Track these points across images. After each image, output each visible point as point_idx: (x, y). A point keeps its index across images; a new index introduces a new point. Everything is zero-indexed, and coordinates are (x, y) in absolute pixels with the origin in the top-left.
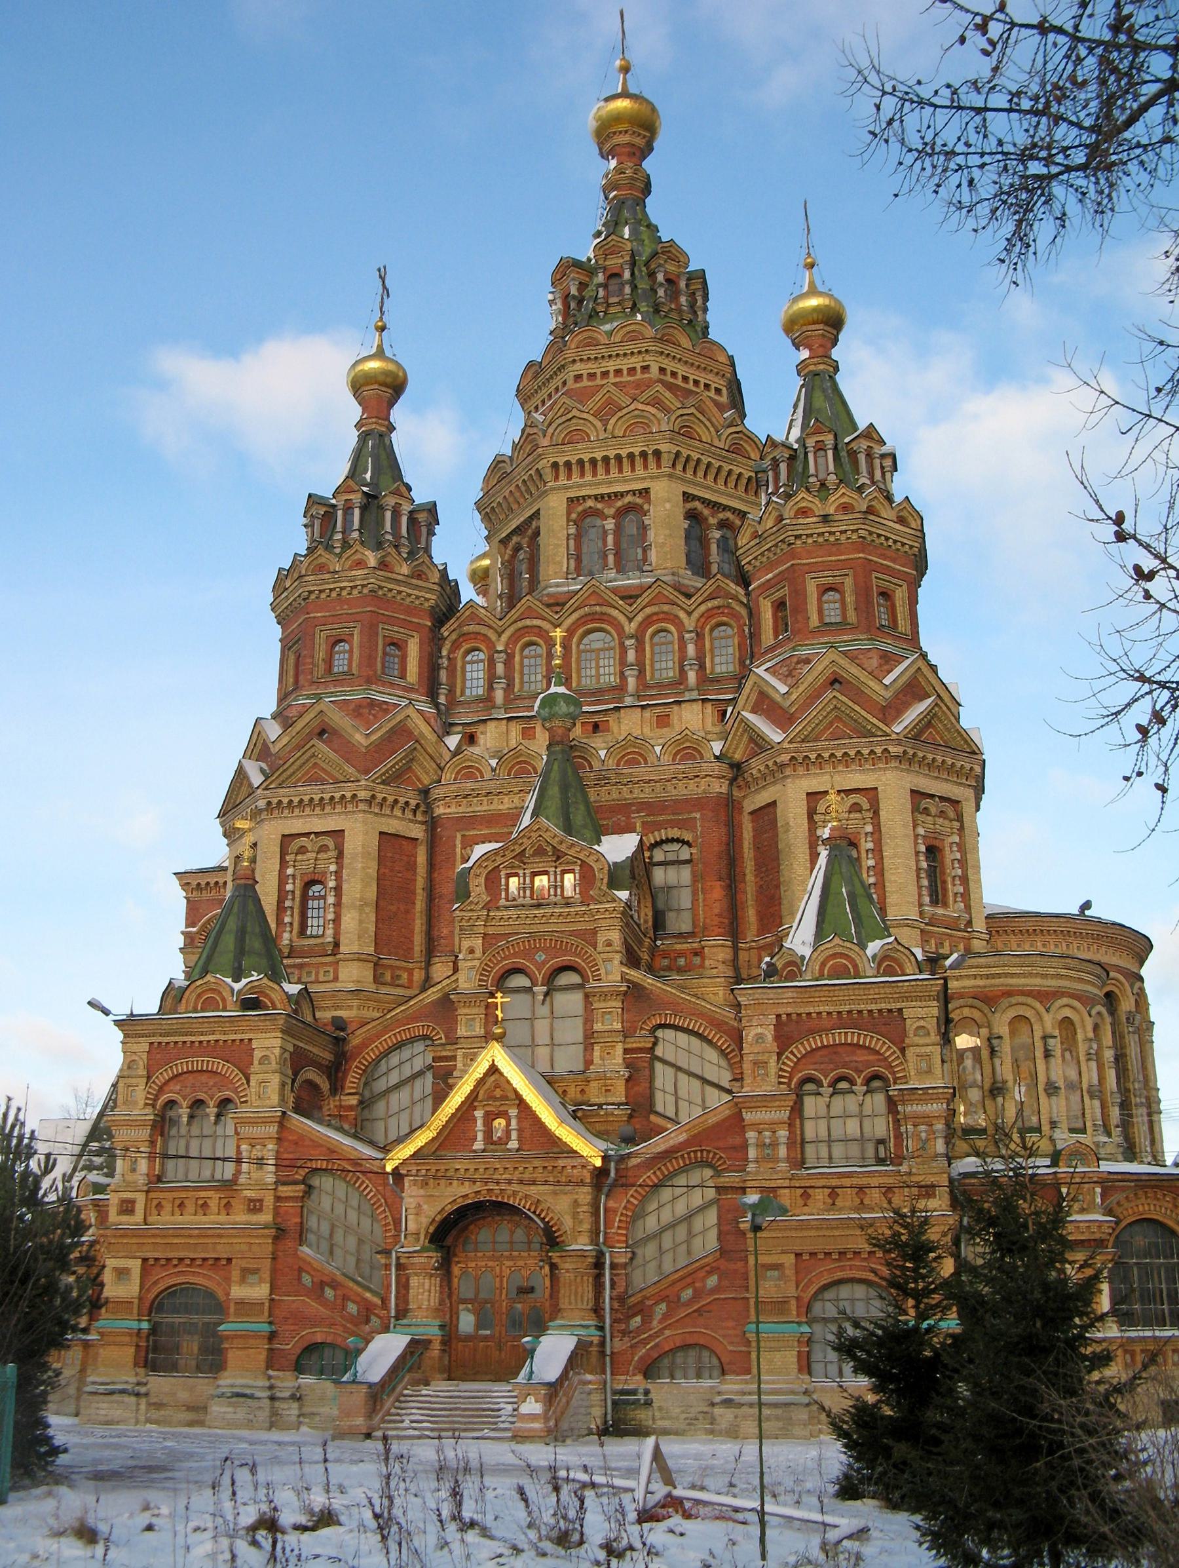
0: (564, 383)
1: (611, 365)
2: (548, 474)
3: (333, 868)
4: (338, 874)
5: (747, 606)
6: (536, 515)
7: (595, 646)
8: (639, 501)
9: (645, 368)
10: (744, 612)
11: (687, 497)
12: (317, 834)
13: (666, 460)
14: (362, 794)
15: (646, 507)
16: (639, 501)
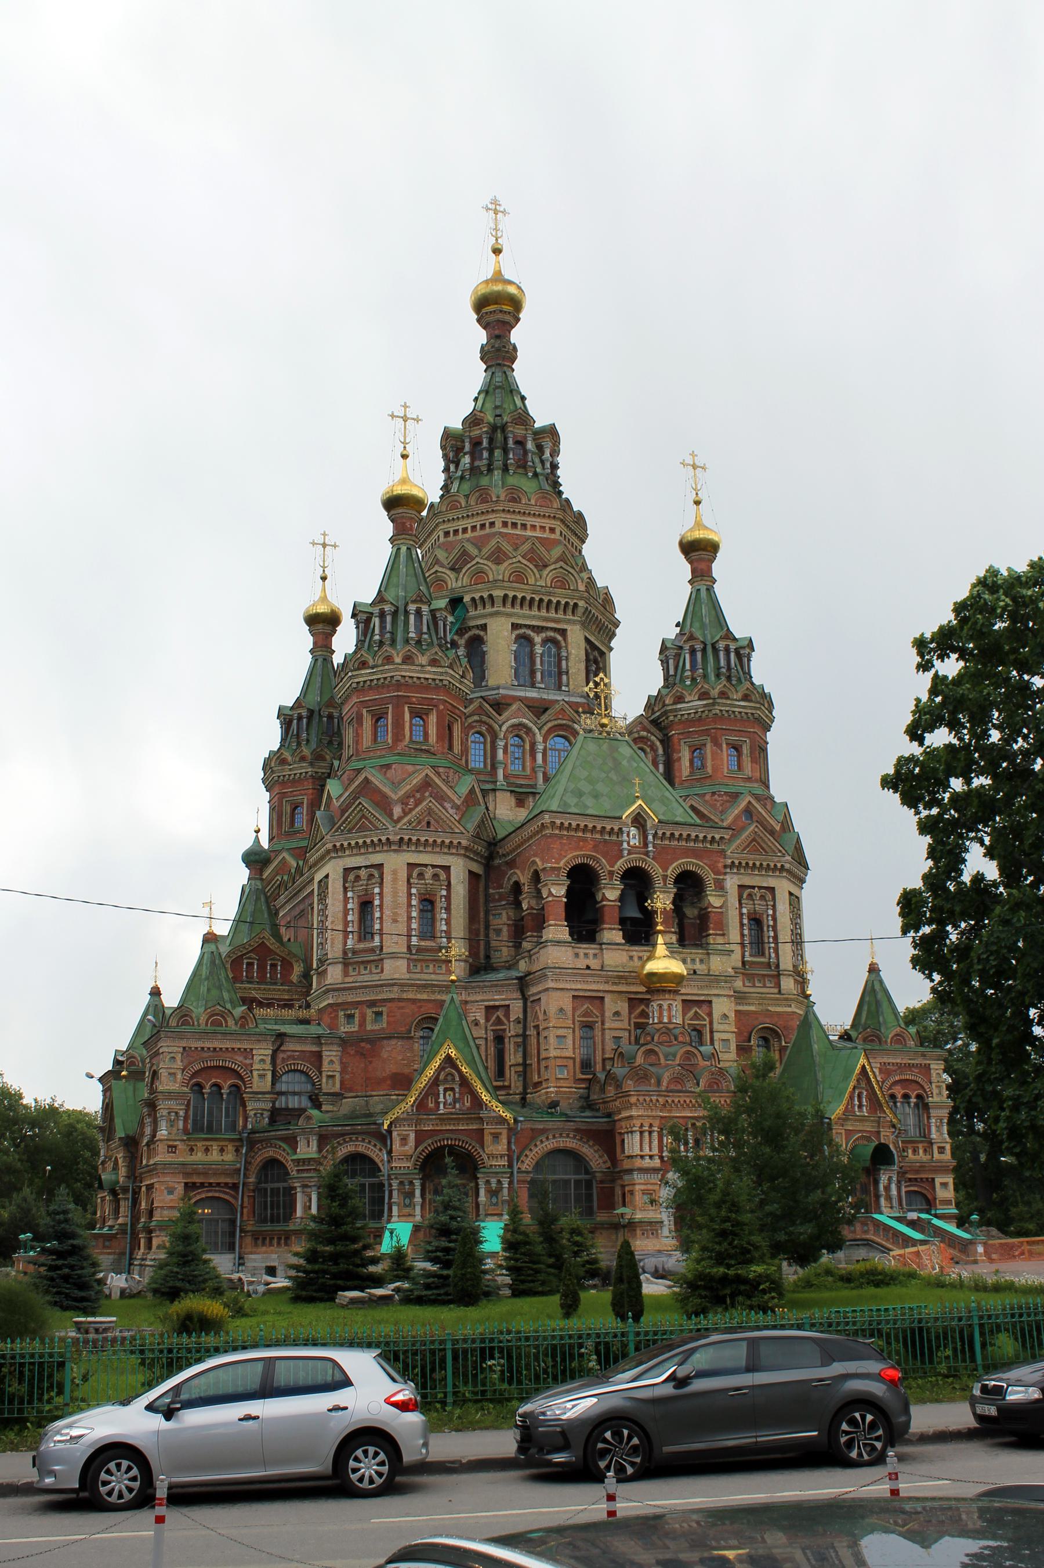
0: (492, 524)
1: (530, 521)
2: (498, 602)
3: (444, 893)
4: (448, 898)
5: (661, 741)
6: (484, 627)
7: (558, 747)
8: (559, 638)
9: (552, 530)
10: (658, 743)
11: (587, 640)
12: (433, 866)
13: (580, 611)
14: (464, 843)
15: (563, 644)
16: (559, 638)
